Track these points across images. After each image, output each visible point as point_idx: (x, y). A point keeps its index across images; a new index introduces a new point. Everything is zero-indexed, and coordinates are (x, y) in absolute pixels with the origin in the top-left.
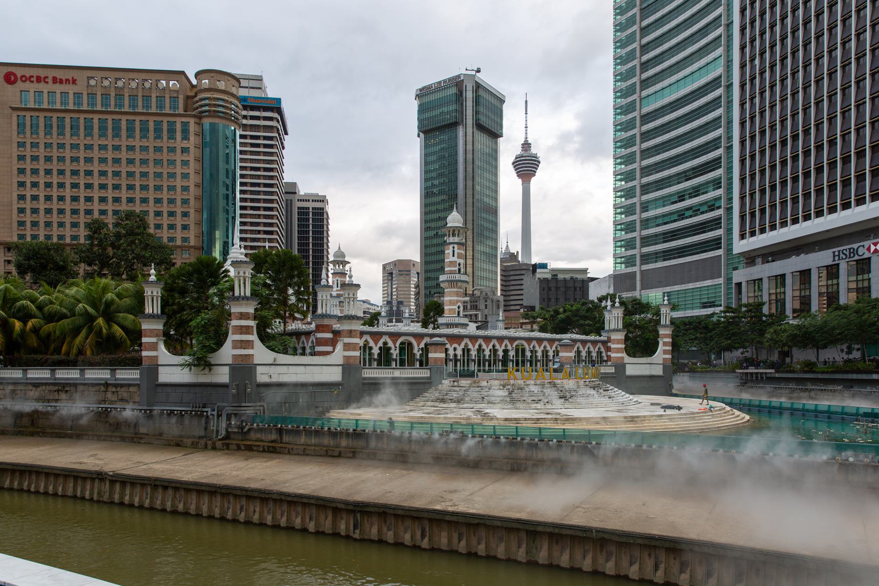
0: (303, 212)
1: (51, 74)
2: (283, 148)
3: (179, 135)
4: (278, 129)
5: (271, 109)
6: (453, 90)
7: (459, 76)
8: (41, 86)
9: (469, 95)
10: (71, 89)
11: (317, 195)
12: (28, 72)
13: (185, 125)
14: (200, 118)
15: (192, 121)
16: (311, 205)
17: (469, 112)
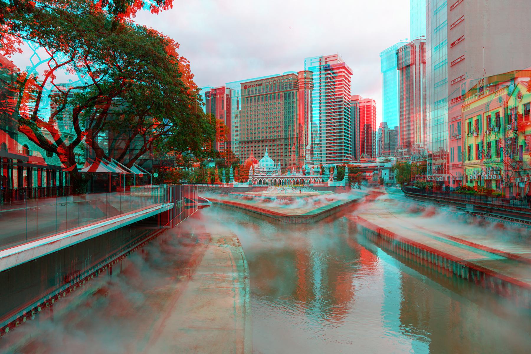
0: (362, 108)
1: (256, 83)
2: (350, 81)
3: (292, 97)
4: (344, 76)
5: (341, 68)
6: (411, 49)
7: (412, 42)
8: (254, 88)
9: (417, 50)
10: (262, 87)
11: (368, 99)
12: (250, 84)
13: (293, 93)
14: (298, 90)
15: (295, 91)
16: (365, 104)
17: (417, 59)
